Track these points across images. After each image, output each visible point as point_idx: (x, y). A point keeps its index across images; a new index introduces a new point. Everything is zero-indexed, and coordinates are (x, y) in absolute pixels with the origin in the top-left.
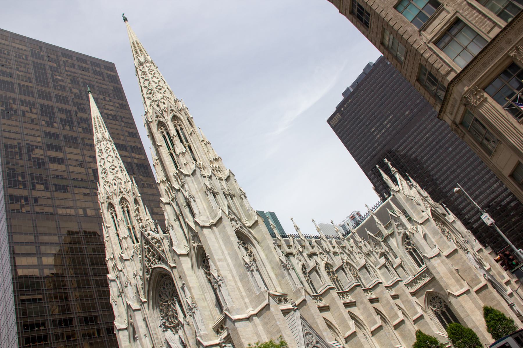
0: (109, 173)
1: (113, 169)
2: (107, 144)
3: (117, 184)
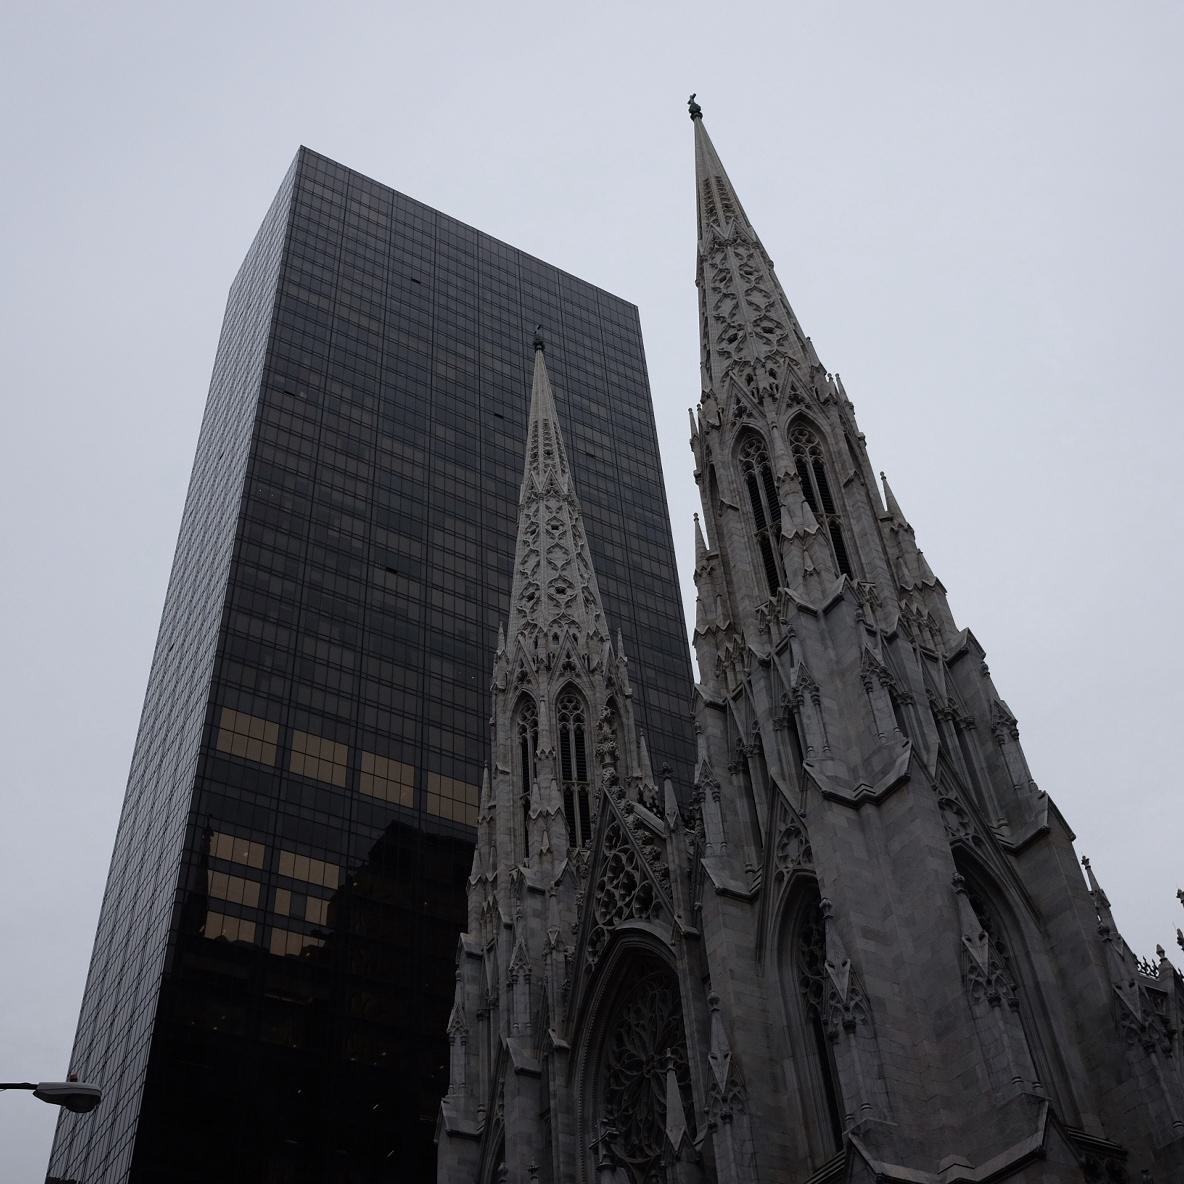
0: (544, 599)
1: (561, 591)
2: (560, 508)
3: (561, 640)
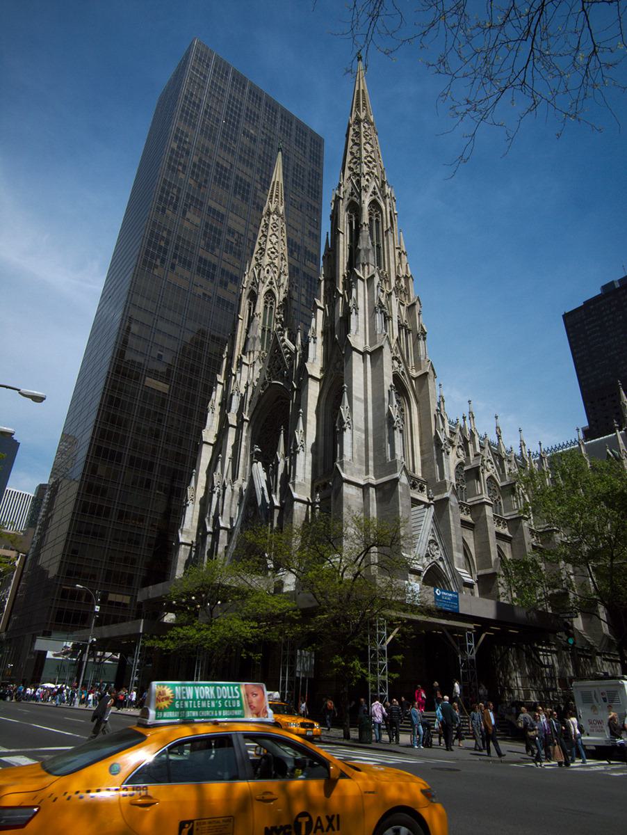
1: (273, 253)
